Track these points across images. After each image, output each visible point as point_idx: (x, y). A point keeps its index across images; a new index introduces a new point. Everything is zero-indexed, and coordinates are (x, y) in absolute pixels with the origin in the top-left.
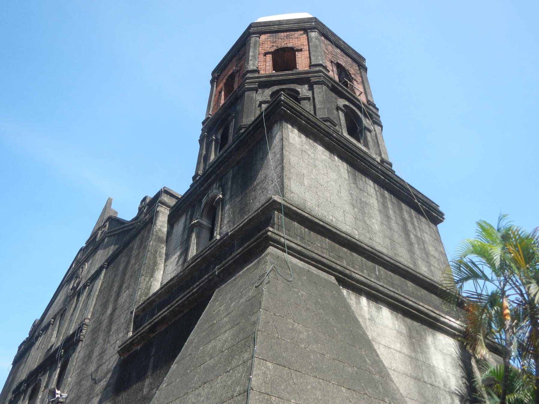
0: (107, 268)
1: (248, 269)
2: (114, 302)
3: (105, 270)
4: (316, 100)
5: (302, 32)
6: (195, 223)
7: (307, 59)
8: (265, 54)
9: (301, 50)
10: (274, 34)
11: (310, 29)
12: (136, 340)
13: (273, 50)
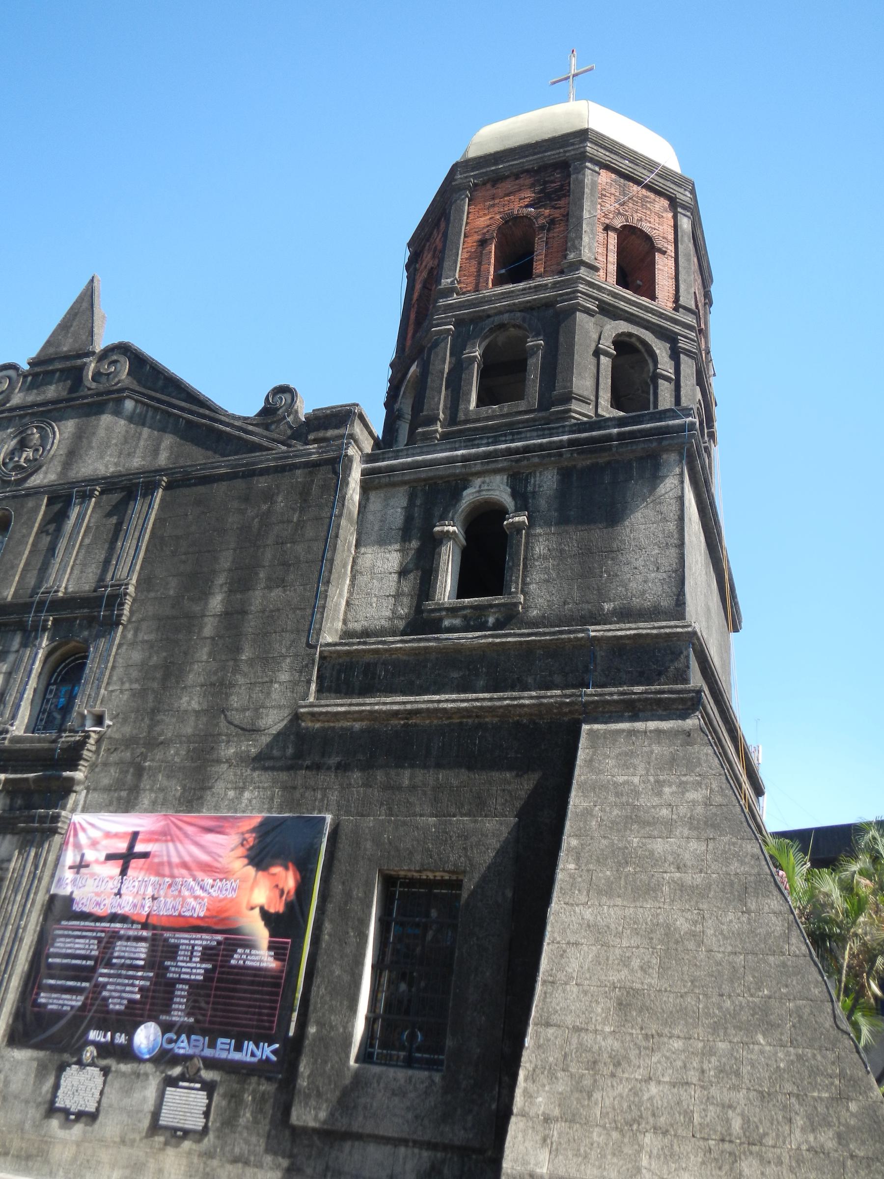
0: (166, 489)
1: (658, 732)
2: (230, 591)
3: (161, 490)
4: (683, 392)
5: (666, 203)
6: (448, 531)
7: (670, 280)
8: (607, 228)
9: (664, 253)
10: (622, 180)
11: (685, 207)
12: (356, 716)
13: (618, 223)
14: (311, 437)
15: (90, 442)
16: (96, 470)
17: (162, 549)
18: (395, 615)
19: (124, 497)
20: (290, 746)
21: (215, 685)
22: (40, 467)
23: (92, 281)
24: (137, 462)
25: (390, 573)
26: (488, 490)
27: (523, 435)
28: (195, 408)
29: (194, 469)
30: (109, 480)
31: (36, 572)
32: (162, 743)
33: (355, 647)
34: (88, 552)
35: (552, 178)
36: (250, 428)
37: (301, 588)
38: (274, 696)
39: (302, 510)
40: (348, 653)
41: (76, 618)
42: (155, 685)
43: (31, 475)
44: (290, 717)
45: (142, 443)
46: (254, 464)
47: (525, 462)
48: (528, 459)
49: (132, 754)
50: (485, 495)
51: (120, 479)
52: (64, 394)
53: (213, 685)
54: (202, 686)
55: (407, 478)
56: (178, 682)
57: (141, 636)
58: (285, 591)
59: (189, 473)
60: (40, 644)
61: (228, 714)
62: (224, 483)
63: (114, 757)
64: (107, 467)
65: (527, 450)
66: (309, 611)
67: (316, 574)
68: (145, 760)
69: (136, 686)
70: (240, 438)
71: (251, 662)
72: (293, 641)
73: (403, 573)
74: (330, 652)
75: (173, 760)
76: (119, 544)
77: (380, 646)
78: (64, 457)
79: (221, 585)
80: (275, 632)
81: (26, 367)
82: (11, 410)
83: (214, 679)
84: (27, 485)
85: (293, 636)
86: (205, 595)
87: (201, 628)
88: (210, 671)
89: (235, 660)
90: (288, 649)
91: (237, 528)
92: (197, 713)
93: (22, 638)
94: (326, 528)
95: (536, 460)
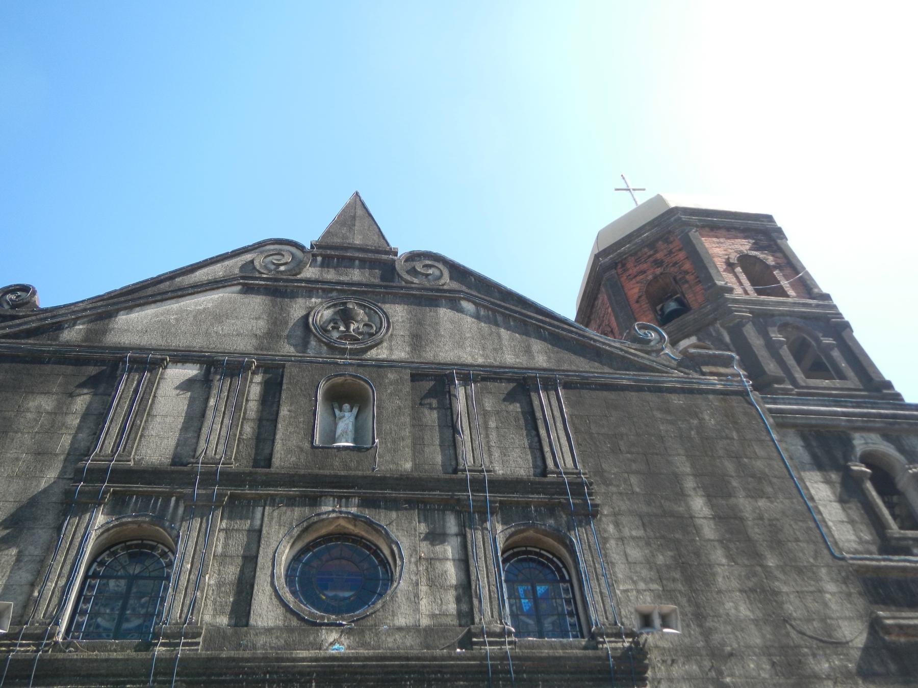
14: (705, 369)
15: (437, 331)
16: (459, 357)
17: (595, 443)
18: (861, 541)
19: (514, 389)
20: (889, 661)
21: (756, 591)
22: (381, 342)
24: (509, 358)
25: (831, 501)
26: (873, 444)
27: (879, 406)
28: (556, 323)
29: (592, 375)
30: (488, 369)
31: (438, 448)
32: (731, 655)
33: (883, 563)
34: (498, 435)
35: (759, 238)
36: (633, 351)
37: (787, 501)
38: (834, 606)
39: (738, 431)
40: (878, 568)
41: (528, 504)
42: (680, 586)
43: (371, 347)
44: (867, 630)
45: (505, 342)
46: (658, 382)
47: (897, 426)
48: (899, 424)
49: (700, 667)
50: (871, 447)
51: (502, 370)
52: (377, 281)
53: (752, 590)
54: (741, 591)
55: (799, 421)
56: (708, 585)
57: (626, 532)
58: (772, 502)
59: (587, 378)
60: (494, 529)
61: (793, 623)
62: (633, 394)
63: (677, 671)
64: (473, 357)
65: (894, 416)
66: (811, 524)
67: (795, 491)
68: (720, 673)
69: (654, 586)
70: (624, 357)
71: (782, 568)
72: (816, 552)
73: (842, 501)
74: (860, 566)
75: (759, 675)
76: (543, 432)
77: (908, 564)
78: (407, 338)
79: (694, 489)
80: (789, 541)
81: (308, 247)
82: (301, 281)
83: (750, 584)
84: (364, 357)
85: (812, 546)
86: (681, 495)
87: (698, 530)
88: (740, 576)
89: (761, 566)
90: (815, 558)
91: (675, 436)
92: (756, 622)
93: (458, 517)
94: (774, 449)
95: (906, 426)
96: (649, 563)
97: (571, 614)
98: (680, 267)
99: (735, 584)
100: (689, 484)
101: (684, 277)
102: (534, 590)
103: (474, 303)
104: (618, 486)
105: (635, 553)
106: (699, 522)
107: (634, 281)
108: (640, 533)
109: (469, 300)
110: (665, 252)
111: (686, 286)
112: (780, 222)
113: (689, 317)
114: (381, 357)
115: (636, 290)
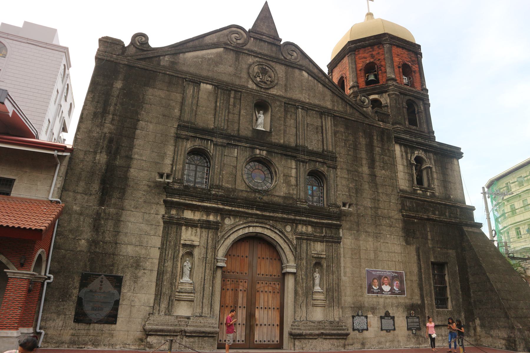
23: (266, 3)
43: (270, 88)
50: (420, 155)
96: (347, 186)
97: (322, 197)
98: (381, 62)
99: (369, 196)
100: (364, 162)
101: (380, 68)
102: (313, 188)
103: (308, 73)
104: (343, 159)
105: (344, 182)
106: (364, 175)
107: (361, 60)
108: (346, 176)
109: (306, 72)
110: (377, 52)
111: (380, 72)
112: (422, 51)
113: (377, 86)
114: (274, 93)
115: (361, 65)
